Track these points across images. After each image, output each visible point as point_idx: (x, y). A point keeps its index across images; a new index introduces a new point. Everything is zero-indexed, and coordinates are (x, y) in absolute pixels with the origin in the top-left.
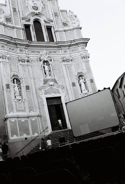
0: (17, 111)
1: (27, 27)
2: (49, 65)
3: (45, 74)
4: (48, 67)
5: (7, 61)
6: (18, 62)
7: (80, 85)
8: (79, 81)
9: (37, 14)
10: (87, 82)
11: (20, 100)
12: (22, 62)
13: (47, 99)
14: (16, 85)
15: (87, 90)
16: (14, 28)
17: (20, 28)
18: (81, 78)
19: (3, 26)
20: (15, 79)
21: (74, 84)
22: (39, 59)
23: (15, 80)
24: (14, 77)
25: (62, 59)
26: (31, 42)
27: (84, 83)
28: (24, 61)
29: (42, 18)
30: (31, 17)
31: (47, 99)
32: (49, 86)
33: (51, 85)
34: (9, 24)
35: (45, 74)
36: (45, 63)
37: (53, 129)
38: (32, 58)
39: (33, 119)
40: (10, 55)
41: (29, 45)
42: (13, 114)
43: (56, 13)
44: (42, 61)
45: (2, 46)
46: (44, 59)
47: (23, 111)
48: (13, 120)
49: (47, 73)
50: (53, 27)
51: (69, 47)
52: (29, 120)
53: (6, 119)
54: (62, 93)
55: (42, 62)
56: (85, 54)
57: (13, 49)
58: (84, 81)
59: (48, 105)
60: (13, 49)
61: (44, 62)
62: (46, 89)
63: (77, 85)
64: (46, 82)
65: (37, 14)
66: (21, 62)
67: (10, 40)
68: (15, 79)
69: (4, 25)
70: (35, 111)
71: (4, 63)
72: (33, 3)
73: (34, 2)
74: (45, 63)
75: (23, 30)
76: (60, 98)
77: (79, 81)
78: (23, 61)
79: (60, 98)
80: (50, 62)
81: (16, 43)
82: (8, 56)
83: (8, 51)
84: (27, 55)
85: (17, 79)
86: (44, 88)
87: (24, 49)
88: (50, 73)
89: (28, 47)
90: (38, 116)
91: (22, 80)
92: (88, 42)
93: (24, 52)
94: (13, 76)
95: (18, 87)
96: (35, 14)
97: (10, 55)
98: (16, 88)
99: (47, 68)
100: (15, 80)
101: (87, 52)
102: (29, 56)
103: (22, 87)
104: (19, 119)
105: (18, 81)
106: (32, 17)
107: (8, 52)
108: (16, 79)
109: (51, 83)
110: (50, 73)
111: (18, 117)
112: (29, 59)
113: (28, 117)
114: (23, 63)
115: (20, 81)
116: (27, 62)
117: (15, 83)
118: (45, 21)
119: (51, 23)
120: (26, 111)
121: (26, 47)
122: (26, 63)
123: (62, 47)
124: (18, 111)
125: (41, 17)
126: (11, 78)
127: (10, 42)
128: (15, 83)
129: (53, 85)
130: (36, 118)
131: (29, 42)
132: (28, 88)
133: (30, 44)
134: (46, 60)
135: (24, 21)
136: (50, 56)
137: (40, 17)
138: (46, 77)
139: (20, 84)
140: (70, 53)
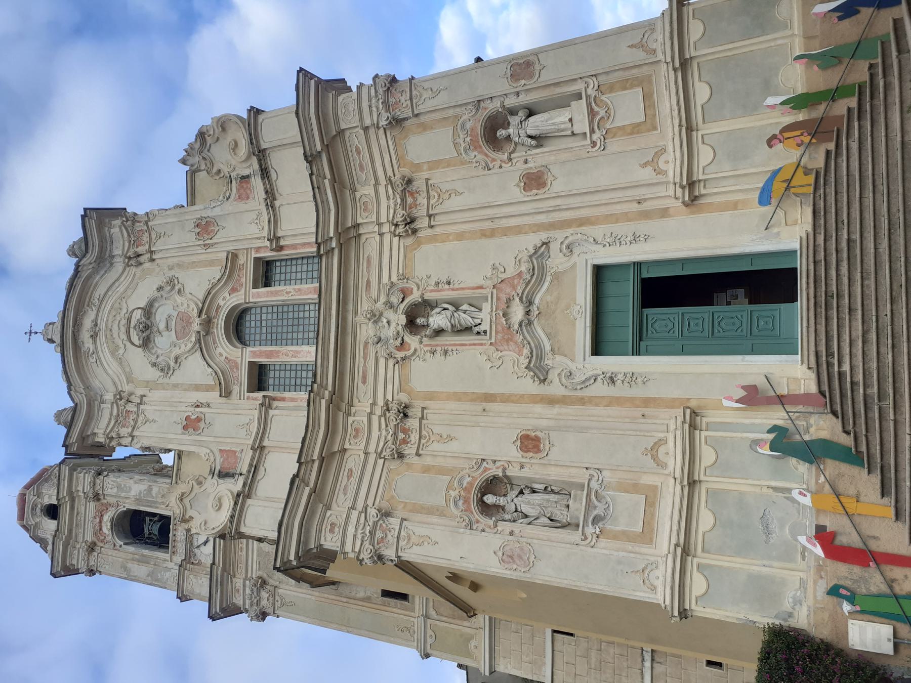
0: (651, 542)
2: (426, 306)
3: (468, 329)
4: (438, 310)
5: (394, 522)
6: (406, 460)
9: (208, 324)
10: (526, 99)
11: (589, 506)
12: (404, 442)
13: (597, 349)
14: (510, 501)
15: (573, 104)
16: (262, 448)
17: (259, 418)
19: (249, 501)
20: (485, 498)
22: (400, 355)
23: (490, 499)
24: (473, 506)
25: (401, 229)
26: (321, 386)
27: (531, 113)
28: (405, 431)
29: (222, 303)
30: (221, 354)
31: (597, 349)
32: (530, 323)
33: (528, 313)
34: (244, 468)
35: (468, 329)
36: (420, 321)
37: (785, 347)
38: (390, 387)
40: (370, 502)
41: (333, 393)
42: (659, 572)
43: (197, 230)
44: (408, 338)
45: (331, 531)
46: (400, 328)
47: (651, 504)
48: (698, 584)
49: (466, 319)
50: (258, 249)
51: (343, 186)
52: (710, 482)
53: (684, 614)
54: (574, 258)
55: (412, 341)
56: (374, 101)
57: (349, 477)
58: (522, 114)
59: (636, 352)
60: (349, 477)
61: (412, 324)
62: (548, 348)
63: (538, 158)
64: (507, 335)
65: (208, 324)
66: (410, 450)
67: (307, 491)
68: (485, 498)
69: (248, 496)
70: (662, 435)
71: (402, 543)
72: (165, 333)
73: (162, 326)
74: (420, 321)
75: (270, 407)
76: (599, 272)
78: (401, 436)
79: (599, 272)
80: (415, 297)
81: (322, 459)
82: (372, 512)
83: (353, 508)
84: (378, 411)
86: (540, 358)
87: (351, 419)
88: (465, 307)
89: (341, 399)
90: (693, 426)
91: (491, 465)
92: (319, 81)
93: (365, 419)
94: (468, 510)
95: (521, 492)
96: (208, 333)
97: (370, 502)
98: (529, 504)
99: (438, 320)
100: (490, 499)
101: (365, 91)
102: (381, 402)
103: (527, 473)
105: (492, 485)
106: (220, 350)
107: (360, 505)
108: (483, 495)
110: (465, 307)
111: (686, 552)
112: (394, 406)
113: (692, 484)
114: (414, 437)
115: (494, 477)
116: (406, 416)
117: (502, 501)
118: (234, 290)
119: (242, 260)
120: (656, 487)
121: (344, 406)
122: (413, 423)
123: (344, 224)
124: (647, 535)
125: (219, 307)
126: (478, 522)
127: (314, 491)
128: (502, 501)
129: (530, 303)
130: (701, 436)
131: (318, 394)
133: (330, 388)
134: (403, 320)
135: (236, 389)
137: (217, 311)
138: (485, 332)
139: (506, 476)
140: (373, 182)
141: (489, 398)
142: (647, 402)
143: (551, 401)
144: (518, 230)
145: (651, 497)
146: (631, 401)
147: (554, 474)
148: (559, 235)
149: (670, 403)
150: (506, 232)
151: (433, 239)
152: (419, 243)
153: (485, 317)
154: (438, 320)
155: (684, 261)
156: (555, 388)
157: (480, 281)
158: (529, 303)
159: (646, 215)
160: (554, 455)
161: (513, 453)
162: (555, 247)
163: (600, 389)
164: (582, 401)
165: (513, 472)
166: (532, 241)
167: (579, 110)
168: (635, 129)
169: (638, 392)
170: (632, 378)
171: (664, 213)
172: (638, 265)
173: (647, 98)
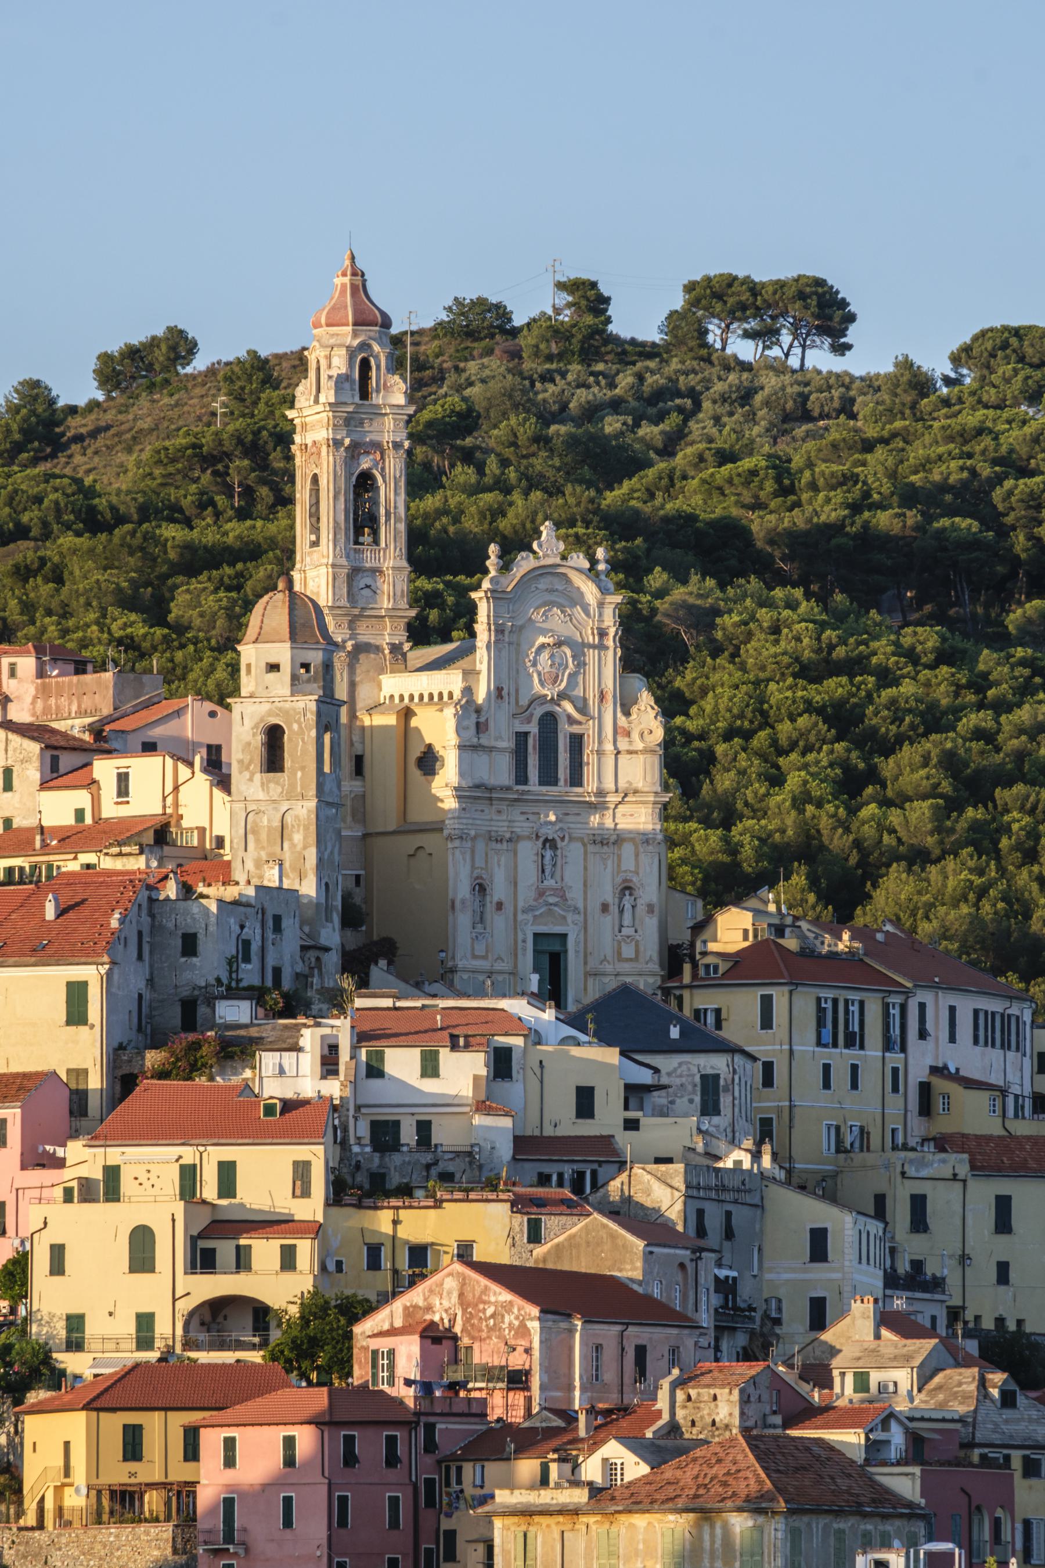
1: (522, 738)
2: (554, 846)
3: (543, 871)
7: (621, 911)
8: (621, 899)
13: (536, 935)
18: (627, 893)
21: (605, 908)
35: (543, 871)
39: (500, 978)
48: (465, 976)
49: (548, 869)
55: (540, 843)
61: (546, 840)
63: (614, 909)
64: (541, 893)
66: (494, 845)
76: (564, 937)
77: (621, 899)
79: (564, 937)
80: (559, 844)
85: (480, 885)
99: (548, 854)
104: (476, 975)
109: (552, 900)
124: (475, 957)
130: (507, 976)
132: (499, 906)
136: (565, 826)
141: (516, 884)
142: (516, 955)
143: (515, 915)
144: (585, 899)
145: (485, 958)
146: (516, 949)
147: (488, 916)
148: (581, 918)
149: (516, 966)
150: (585, 893)
151: (586, 853)
152: (584, 845)
153: (550, 883)
154: (548, 854)
155: (566, 969)
156: (520, 917)
157: (566, 879)
158: (555, 905)
159: (585, 956)
160: (496, 917)
161: (496, 899)
162: (577, 917)
163: (520, 936)
164: (516, 928)
165: (488, 898)
166: (580, 905)
167: (630, 931)
168: (619, 953)
169: (520, 952)
170: (524, 949)
171: (585, 963)
172: (566, 951)
173: (631, 960)
